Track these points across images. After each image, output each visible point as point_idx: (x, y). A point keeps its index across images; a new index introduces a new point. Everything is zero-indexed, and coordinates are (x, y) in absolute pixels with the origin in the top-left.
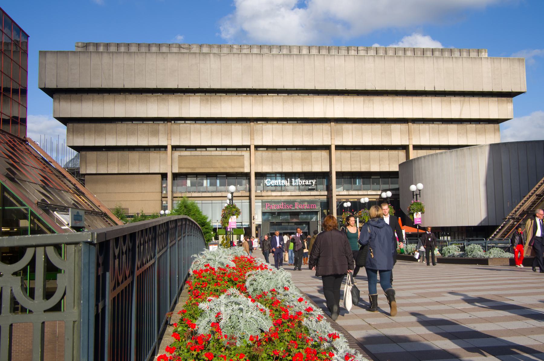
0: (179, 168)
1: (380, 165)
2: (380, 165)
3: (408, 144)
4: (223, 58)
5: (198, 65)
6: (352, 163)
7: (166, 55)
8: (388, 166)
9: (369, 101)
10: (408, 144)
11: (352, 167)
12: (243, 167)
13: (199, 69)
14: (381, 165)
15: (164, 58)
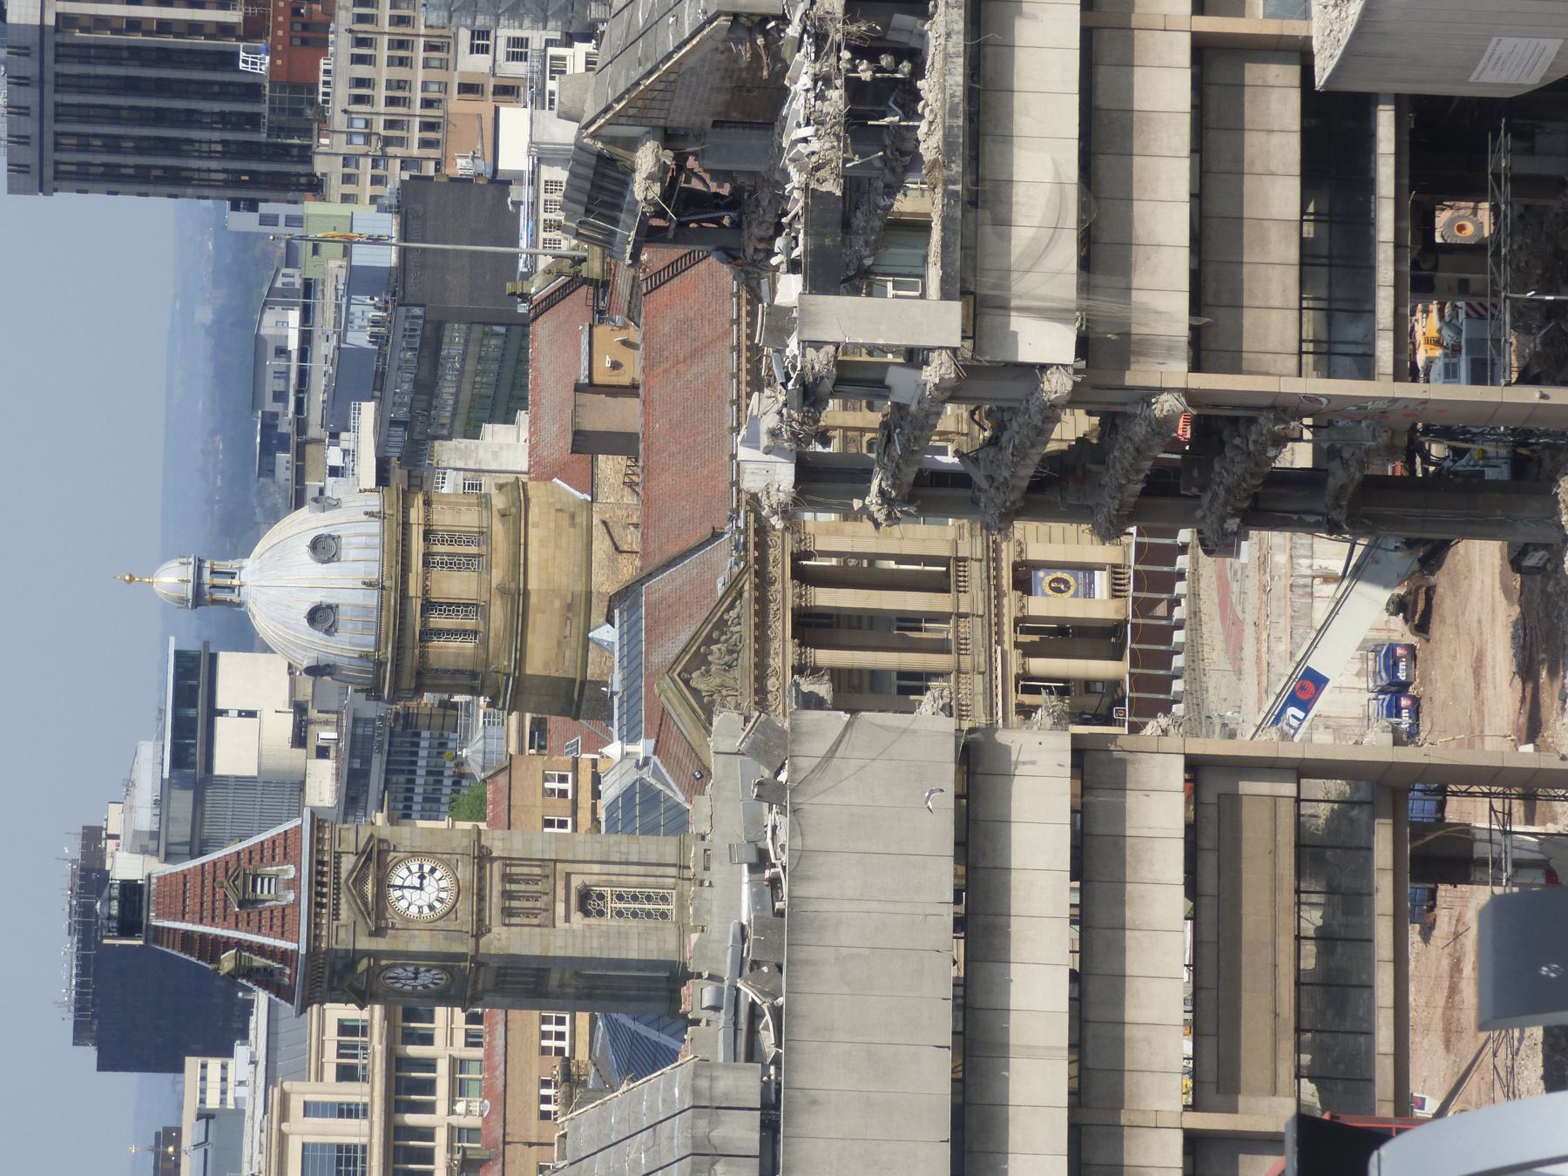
0: (1275, 1093)
1: (1272, 174)
2: (1272, 174)
3: (1189, 35)
4: (812, 842)
5: (844, 951)
6: (1262, 304)
7: (798, 1093)
8: (1276, 139)
9: (1001, 202)
10: (1187, 38)
11: (1277, 304)
12: (1275, 798)
13: (867, 952)
14: (1273, 169)
15: (814, 1102)
